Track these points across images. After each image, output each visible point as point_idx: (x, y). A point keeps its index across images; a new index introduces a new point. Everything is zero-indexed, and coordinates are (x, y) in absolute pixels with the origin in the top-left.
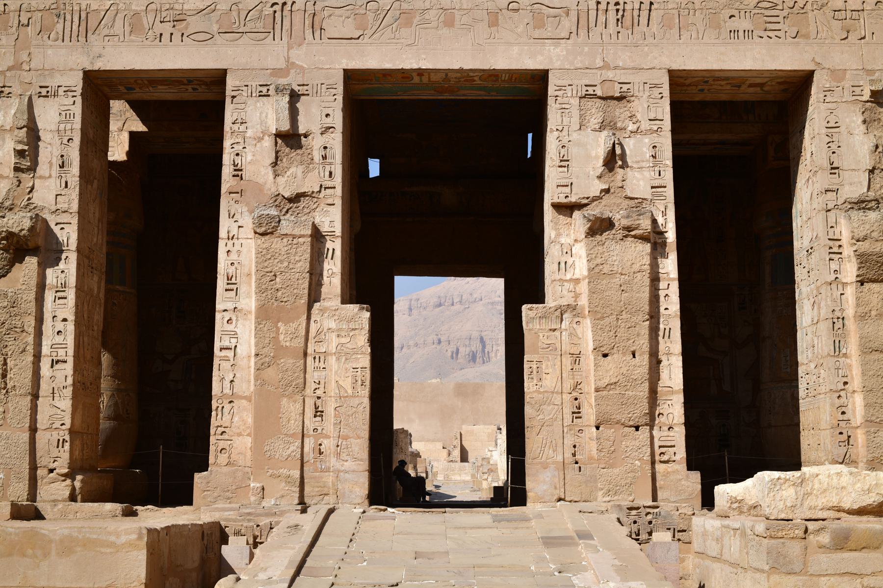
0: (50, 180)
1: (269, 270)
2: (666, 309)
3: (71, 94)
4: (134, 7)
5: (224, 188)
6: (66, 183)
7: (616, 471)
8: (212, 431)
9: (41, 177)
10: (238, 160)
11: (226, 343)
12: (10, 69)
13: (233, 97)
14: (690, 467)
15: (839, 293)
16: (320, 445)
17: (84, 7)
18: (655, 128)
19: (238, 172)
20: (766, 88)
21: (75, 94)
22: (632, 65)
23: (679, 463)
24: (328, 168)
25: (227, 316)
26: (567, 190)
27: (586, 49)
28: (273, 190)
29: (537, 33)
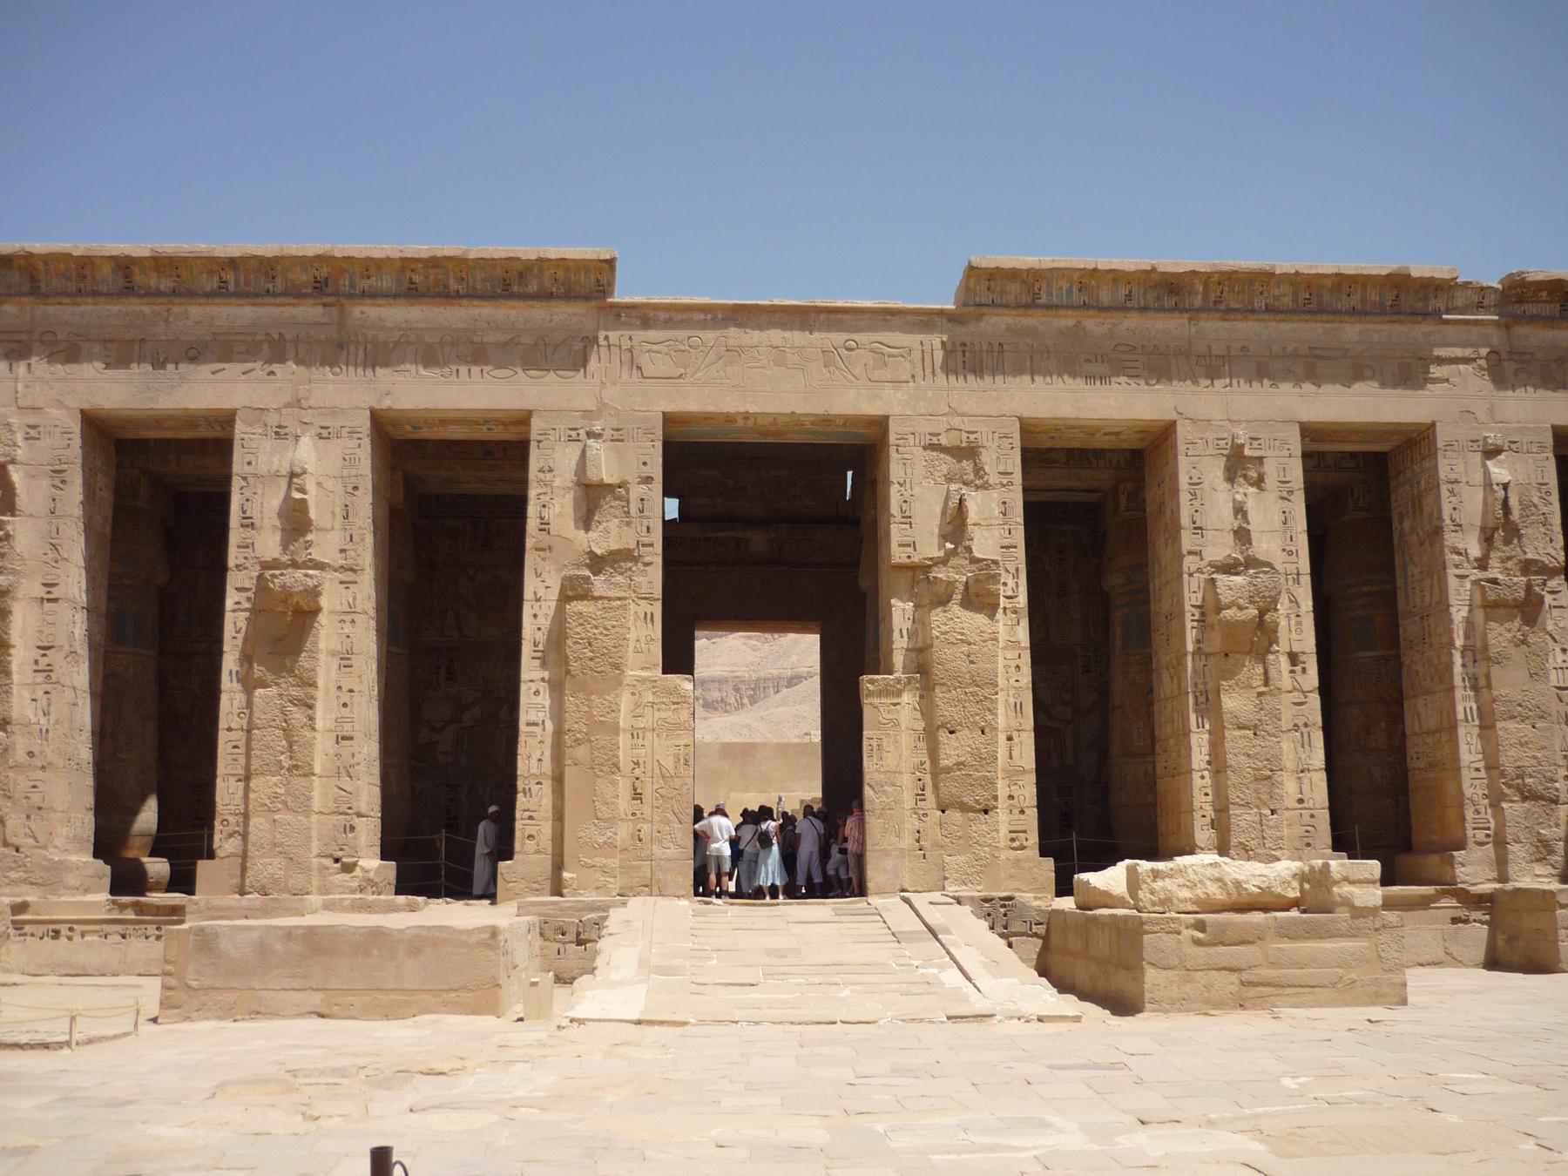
0: (332, 532)
1: (583, 635)
2: (1017, 681)
3: (355, 436)
4: (427, 339)
5: (530, 543)
6: (351, 536)
7: (961, 858)
8: (518, 815)
9: (323, 529)
10: (545, 513)
11: (533, 718)
12: (288, 405)
13: (539, 442)
14: (1043, 853)
15: (1202, 664)
16: (639, 831)
17: (370, 338)
18: (1005, 482)
19: (544, 526)
20: (1121, 437)
21: (360, 436)
22: (980, 412)
23: (1031, 848)
24: (645, 522)
25: (534, 687)
26: (910, 549)
27: (930, 393)
28: (585, 546)
29: (876, 375)
